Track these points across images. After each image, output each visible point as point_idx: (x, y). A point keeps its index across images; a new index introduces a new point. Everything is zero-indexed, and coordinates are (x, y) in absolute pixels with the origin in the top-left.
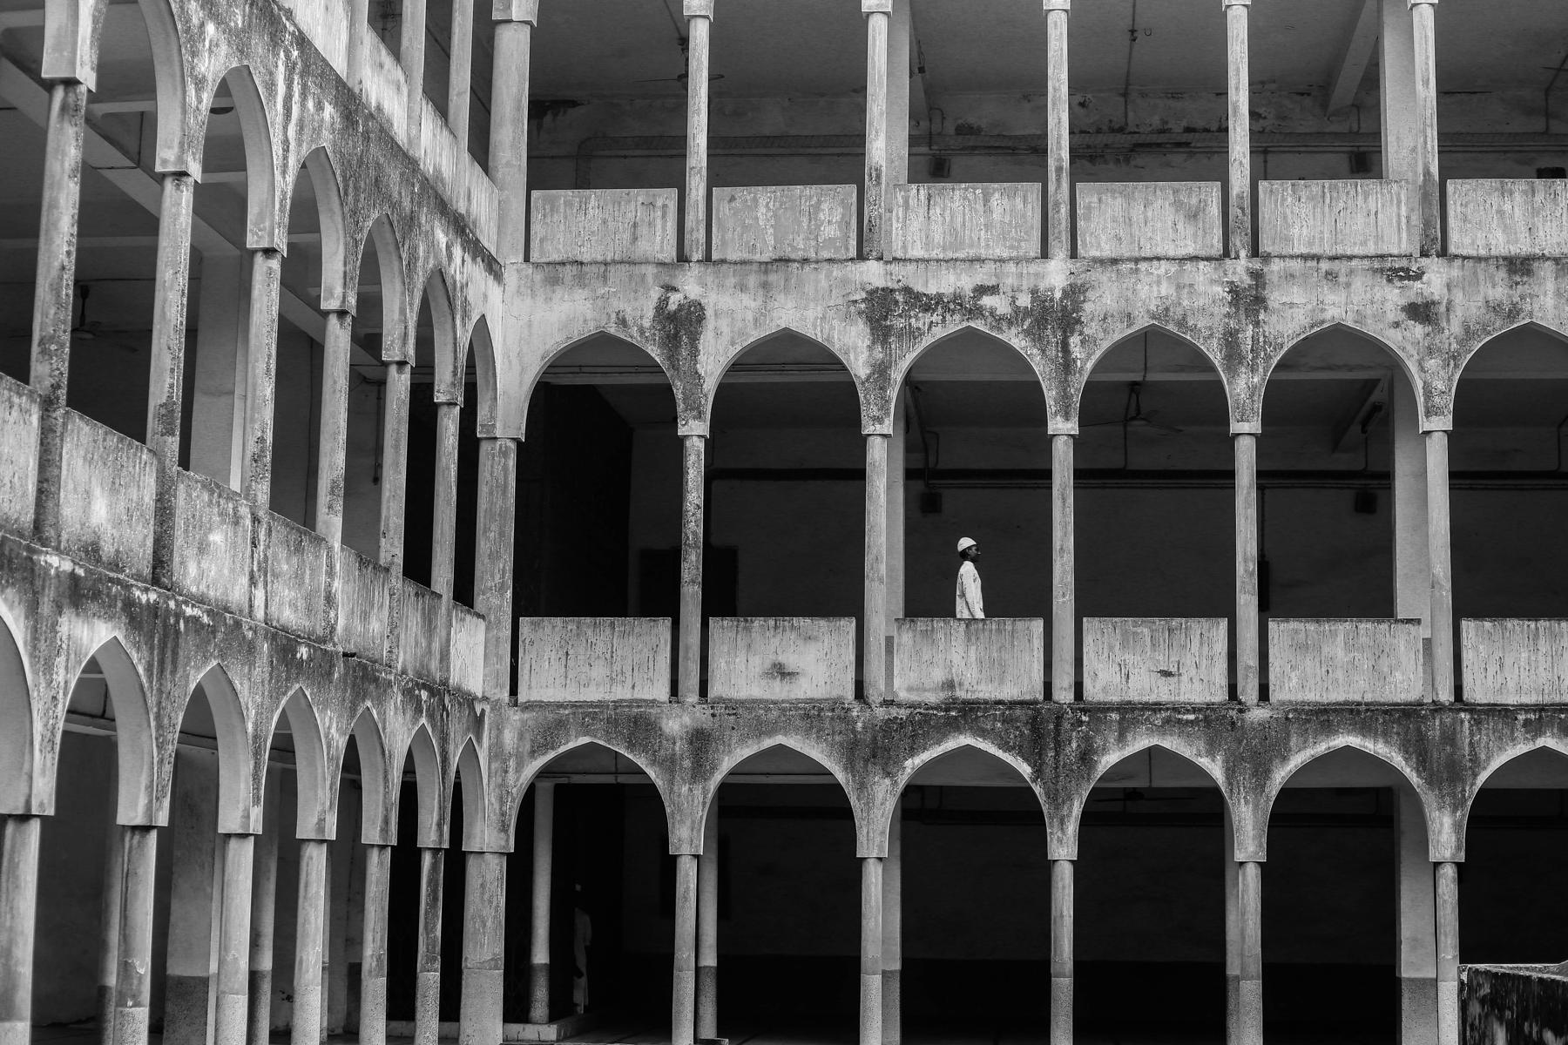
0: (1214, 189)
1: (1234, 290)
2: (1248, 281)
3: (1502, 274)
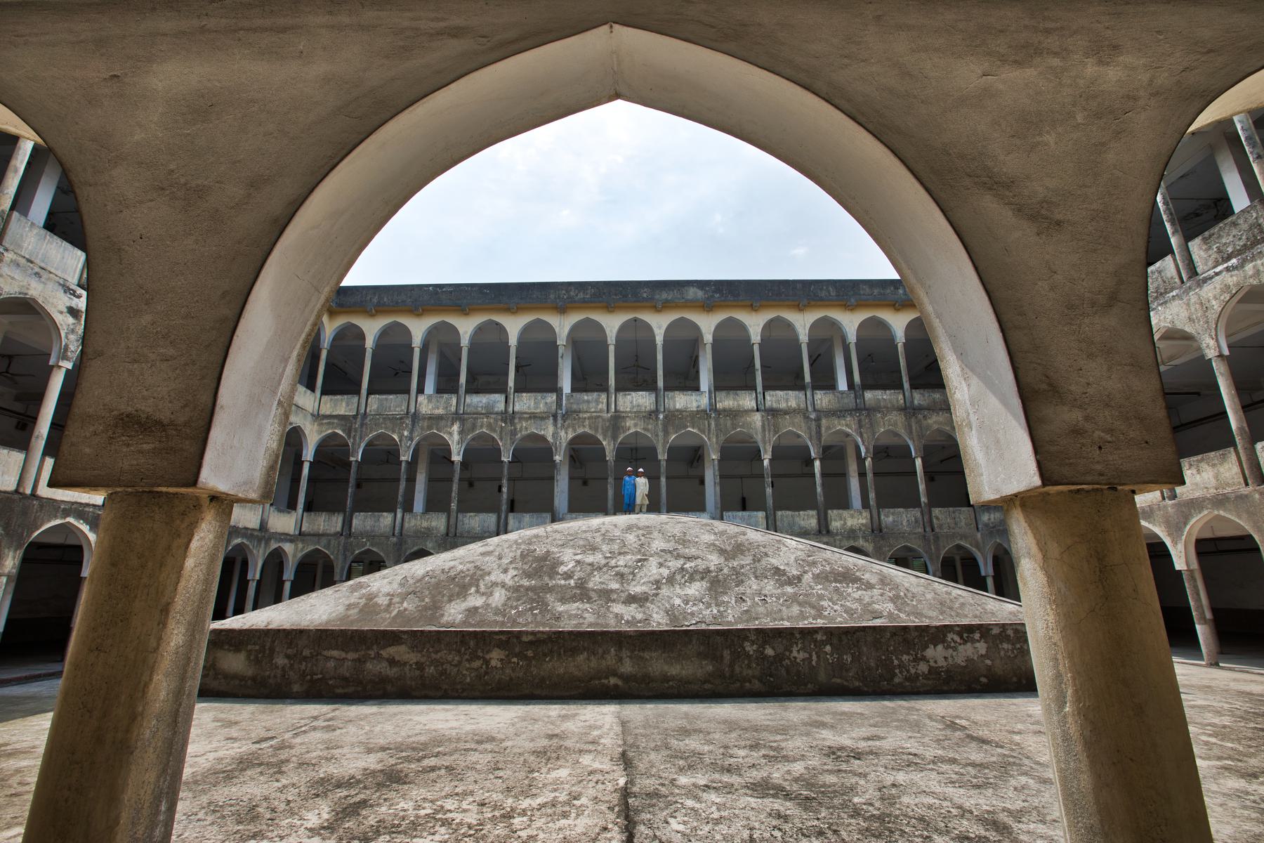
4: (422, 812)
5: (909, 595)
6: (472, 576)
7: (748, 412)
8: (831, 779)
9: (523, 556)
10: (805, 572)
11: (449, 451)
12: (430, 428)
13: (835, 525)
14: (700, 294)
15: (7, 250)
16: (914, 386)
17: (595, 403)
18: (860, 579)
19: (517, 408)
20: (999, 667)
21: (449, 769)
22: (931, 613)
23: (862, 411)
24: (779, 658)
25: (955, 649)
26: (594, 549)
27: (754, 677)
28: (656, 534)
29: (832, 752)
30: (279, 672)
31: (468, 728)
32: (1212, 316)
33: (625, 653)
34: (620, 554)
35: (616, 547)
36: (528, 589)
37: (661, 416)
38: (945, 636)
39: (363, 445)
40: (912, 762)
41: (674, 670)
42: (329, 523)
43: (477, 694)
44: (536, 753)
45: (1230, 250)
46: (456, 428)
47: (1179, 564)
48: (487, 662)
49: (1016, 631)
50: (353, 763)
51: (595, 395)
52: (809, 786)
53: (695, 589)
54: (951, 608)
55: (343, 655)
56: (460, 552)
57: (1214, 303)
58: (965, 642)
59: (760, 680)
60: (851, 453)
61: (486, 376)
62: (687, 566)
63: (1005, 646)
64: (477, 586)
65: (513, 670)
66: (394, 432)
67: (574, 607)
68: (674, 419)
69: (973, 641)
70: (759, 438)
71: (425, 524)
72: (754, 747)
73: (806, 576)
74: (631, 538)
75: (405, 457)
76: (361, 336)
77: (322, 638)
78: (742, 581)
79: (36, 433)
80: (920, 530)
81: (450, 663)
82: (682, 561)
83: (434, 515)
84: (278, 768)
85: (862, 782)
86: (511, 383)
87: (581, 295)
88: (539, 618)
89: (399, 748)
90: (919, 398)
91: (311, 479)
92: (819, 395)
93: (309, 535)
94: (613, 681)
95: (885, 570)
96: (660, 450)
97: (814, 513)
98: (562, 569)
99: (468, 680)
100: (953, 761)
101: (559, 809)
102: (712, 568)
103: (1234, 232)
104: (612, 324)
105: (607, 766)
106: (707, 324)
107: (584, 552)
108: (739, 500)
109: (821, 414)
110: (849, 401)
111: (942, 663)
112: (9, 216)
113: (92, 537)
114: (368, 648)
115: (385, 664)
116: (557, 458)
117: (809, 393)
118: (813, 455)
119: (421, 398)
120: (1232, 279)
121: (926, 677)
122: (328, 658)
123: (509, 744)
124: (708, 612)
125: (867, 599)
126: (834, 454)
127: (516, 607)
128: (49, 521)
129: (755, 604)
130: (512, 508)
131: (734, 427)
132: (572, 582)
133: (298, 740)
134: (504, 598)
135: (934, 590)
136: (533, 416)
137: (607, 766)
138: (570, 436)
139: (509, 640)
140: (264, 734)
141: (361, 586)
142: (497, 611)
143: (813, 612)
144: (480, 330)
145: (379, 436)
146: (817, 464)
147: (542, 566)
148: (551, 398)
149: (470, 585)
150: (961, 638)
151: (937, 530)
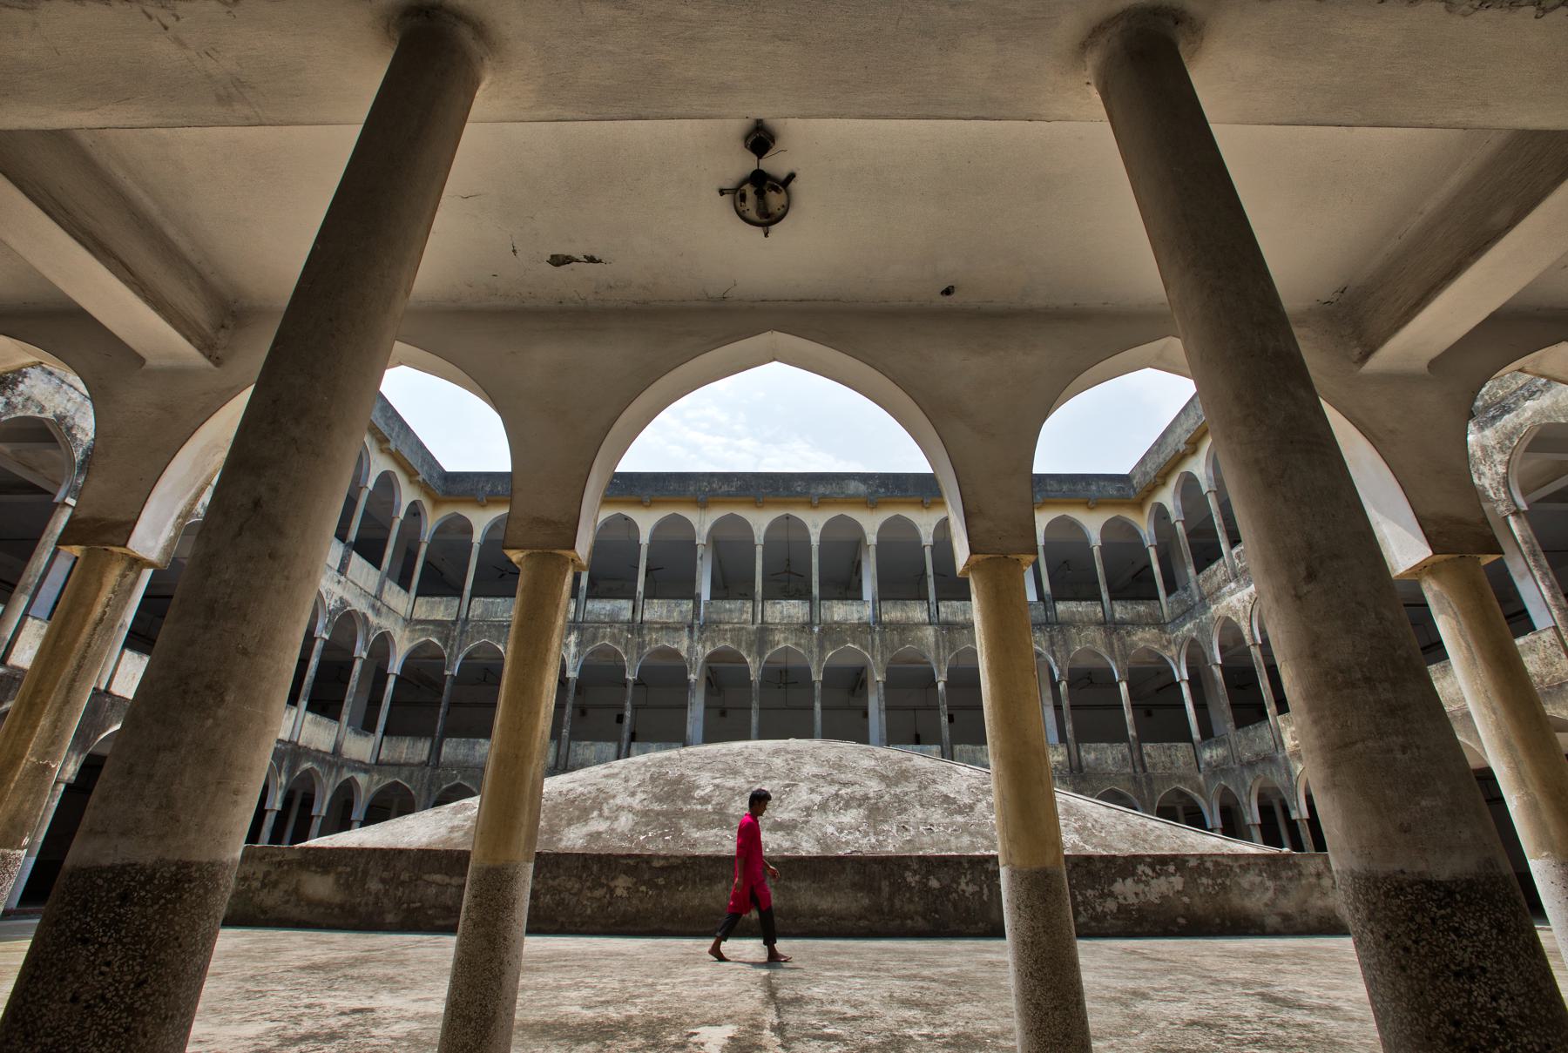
5: (1098, 826)
7: (918, 625)
14: (862, 488)
17: (738, 612)
19: (647, 617)
20: (1199, 905)
22: (1121, 846)
23: (1053, 624)
24: (945, 891)
25: (1147, 884)
26: (735, 772)
27: (916, 913)
28: (807, 758)
29: (992, 964)
30: (371, 899)
36: (658, 814)
37: (816, 629)
38: (1135, 868)
39: (461, 656)
41: (825, 903)
42: (413, 750)
43: (599, 928)
48: (611, 891)
49: (1216, 864)
53: (851, 816)
54: (1145, 841)
55: (447, 880)
56: (580, 774)
58: (1158, 875)
59: (924, 918)
63: (1204, 880)
64: (601, 810)
66: (499, 641)
67: (711, 834)
68: (832, 633)
69: (1168, 875)
70: (931, 656)
72: (912, 960)
74: (778, 762)
76: (468, 529)
77: (425, 859)
80: (1129, 770)
81: (568, 891)
82: (836, 787)
86: (640, 587)
87: (725, 488)
88: (671, 845)
90: (1120, 611)
95: (1071, 800)
96: (814, 669)
98: (698, 793)
99: (589, 911)
104: (760, 521)
106: (871, 523)
108: (910, 730)
111: (1132, 900)
116: (692, 677)
121: (1115, 917)
122: (429, 884)
127: (645, 833)
130: (633, 738)
132: (710, 807)
134: (631, 823)
136: (665, 627)
138: (708, 651)
139: (637, 865)
141: (465, 808)
142: (623, 837)
143: (986, 843)
147: (676, 790)
148: (687, 605)
149: (593, 809)
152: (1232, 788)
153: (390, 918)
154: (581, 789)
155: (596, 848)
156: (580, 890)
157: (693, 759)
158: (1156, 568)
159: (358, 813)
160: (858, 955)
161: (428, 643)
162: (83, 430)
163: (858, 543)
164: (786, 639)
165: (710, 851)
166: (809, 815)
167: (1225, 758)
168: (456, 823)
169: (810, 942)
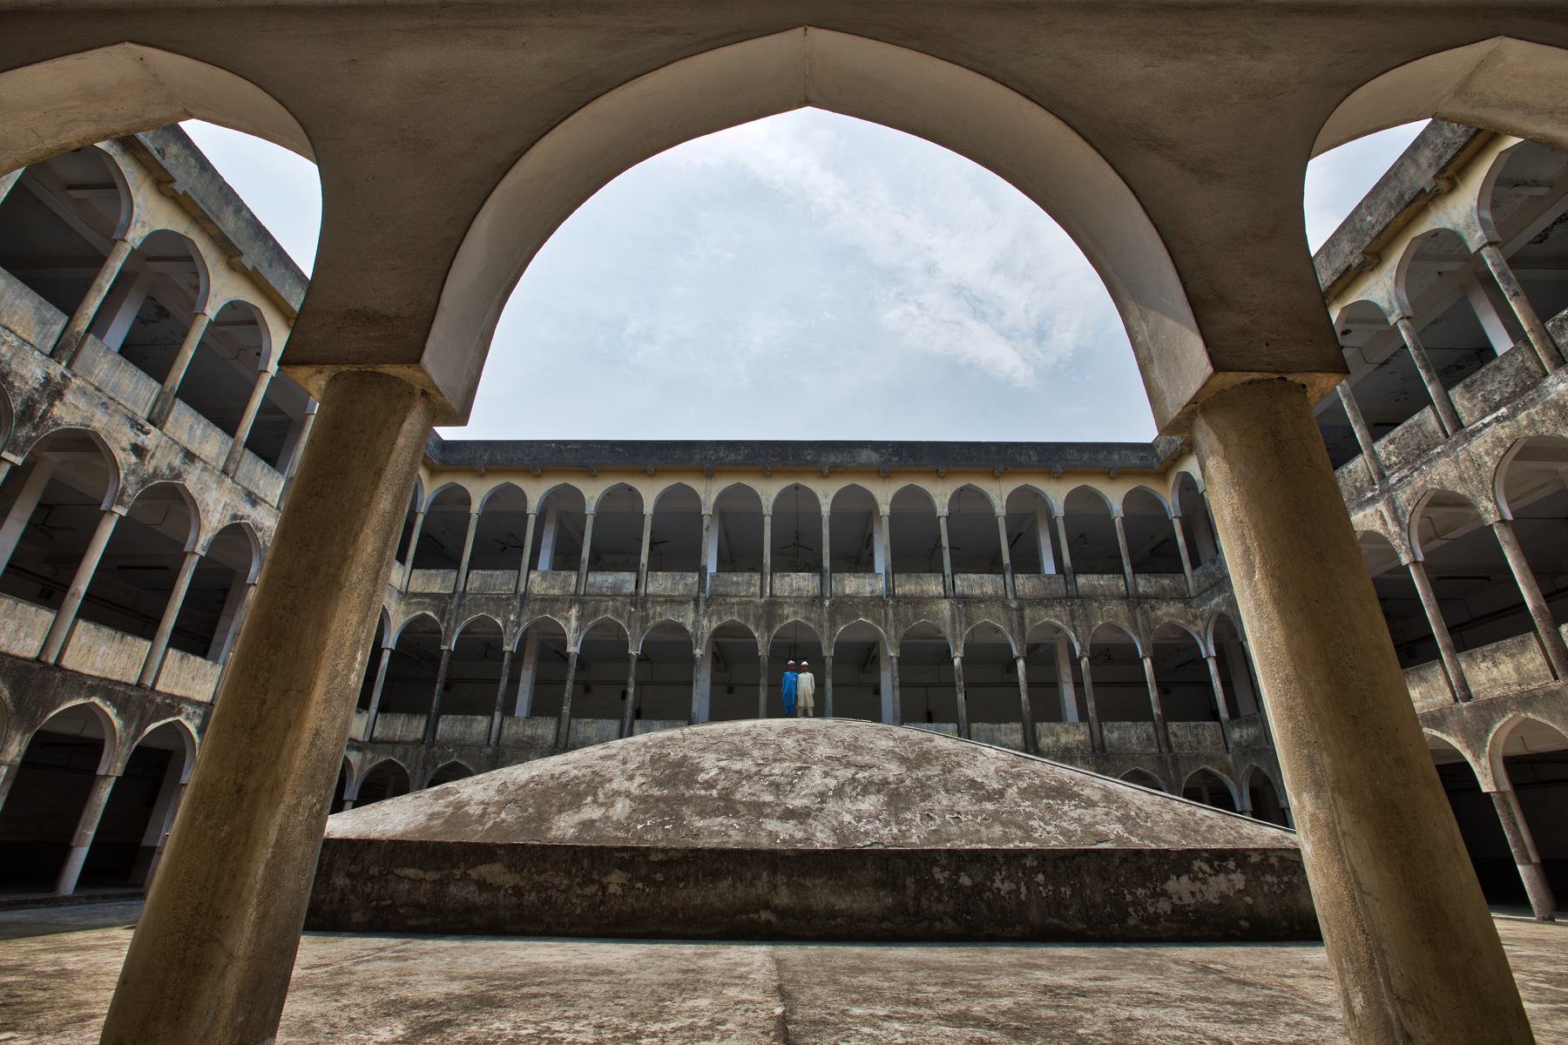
0: (63, 320)
1: (48, 379)
2: (59, 379)
3: (181, 455)
4: (523, 1032)
5: (1142, 815)
6: (589, 784)
8: (1044, 1013)
9: (653, 761)
10: (1009, 786)
11: (563, 643)
12: (542, 611)
13: (1046, 742)
14: (875, 457)
15: (75, 376)
16: (1137, 569)
17: (745, 585)
18: (1079, 795)
19: (650, 590)
21: (557, 997)
22: (1171, 837)
23: (1074, 599)
24: (978, 889)
25: (1204, 881)
26: (742, 754)
28: (820, 738)
29: (1049, 990)
31: (578, 962)
32: (1487, 474)
33: (781, 879)
34: (775, 760)
35: (770, 752)
36: (658, 799)
38: (1190, 864)
39: (458, 631)
40: (1153, 1000)
41: (843, 903)
42: (408, 728)
44: (668, 985)
45: (1497, 397)
46: (574, 612)
47: (1486, 786)
48: (604, 888)
49: (1282, 859)
50: (436, 989)
51: (747, 575)
52: (1019, 1018)
53: (868, 804)
55: (421, 874)
56: (575, 755)
57: (1487, 459)
58: (1217, 872)
59: (954, 919)
60: (1062, 651)
61: (614, 551)
62: (860, 776)
63: (1269, 878)
64: (595, 795)
65: (637, 898)
66: (497, 615)
67: (716, 822)
68: (844, 606)
69: (1228, 871)
70: (947, 631)
71: (529, 732)
72: (950, 983)
73: (1010, 791)
74: (789, 742)
75: (509, 647)
76: (467, 501)
78: (929, 796)
79: (72, 590)
81: (557, 888)
82: (852, 770)
83: (539, 719)
84: (338, 991)
85: (1089, 1016)
86: (644, 559)
87: (732, 457)
88: (672, 835)
89: (490, 977)
90: (1144, 584)
91: (389, 677)
92: (1021, 579)
93: (382, 742)
94: (765, 915)
96: (825, 644)
97: (1018, 726)
98: (702, 777)
99: (579, 911)
100: (1207, 1000)
101: (699, 1032)
102: (891, 779)
103: (1499, 377)
104: (768, 491)
105: (758, 997)
106: (884, 494)
107: (730, 758)
109: (1025, 603)
110: (1059, 587)
111: (1188, 899)
112: (84, 338)
113: (118, 723)
114: (454, 867)
115: (473, 888)
116: (698, 652)
117: (1008, 577)
118: (1015, 653)
119: (533, 575)
120: (1503, 431)
122: (401, 878)
123: (632, 976)
124: (886, 831)
125: (1088, 819)
126: (1042, 655)
127: (644, 821)
128: (70, 699)
129: (945, 823)
130: (638, 714)
131: (917, 617)
132: (715, 793)
133: (360, 967)
134: (628, 810)
135: (1173, 810)
136: (670, 600)
137: (758, 997)
138: (714, 625)
139: (631, 859)
140: (315, 961)
141: (448, 792)
142: (619, 826)
143: (1020, 833)
144: (608, 496)
145: (478, 620)
146: (1021, 664)
147: (679, 773)
148: (693, 578)
149: (586, 794)
150: (1212, 867)
151: (1176, 750)
152: (1265, 770)
153: (357, 917)
154: (575, 772)
155: (589, 840)
156: (569, 887)
157: (698, 739)
158: (1180, 540)
159: (351, 792)
160: (886, 973)
161: (425, 616)
162: (22, 377)
163: (871, 513)
164: (795, 613)
165: (714, 842)
166: (823, 802)
167: (1257, 738)
168: (436, 809)
169: (827, 949)
